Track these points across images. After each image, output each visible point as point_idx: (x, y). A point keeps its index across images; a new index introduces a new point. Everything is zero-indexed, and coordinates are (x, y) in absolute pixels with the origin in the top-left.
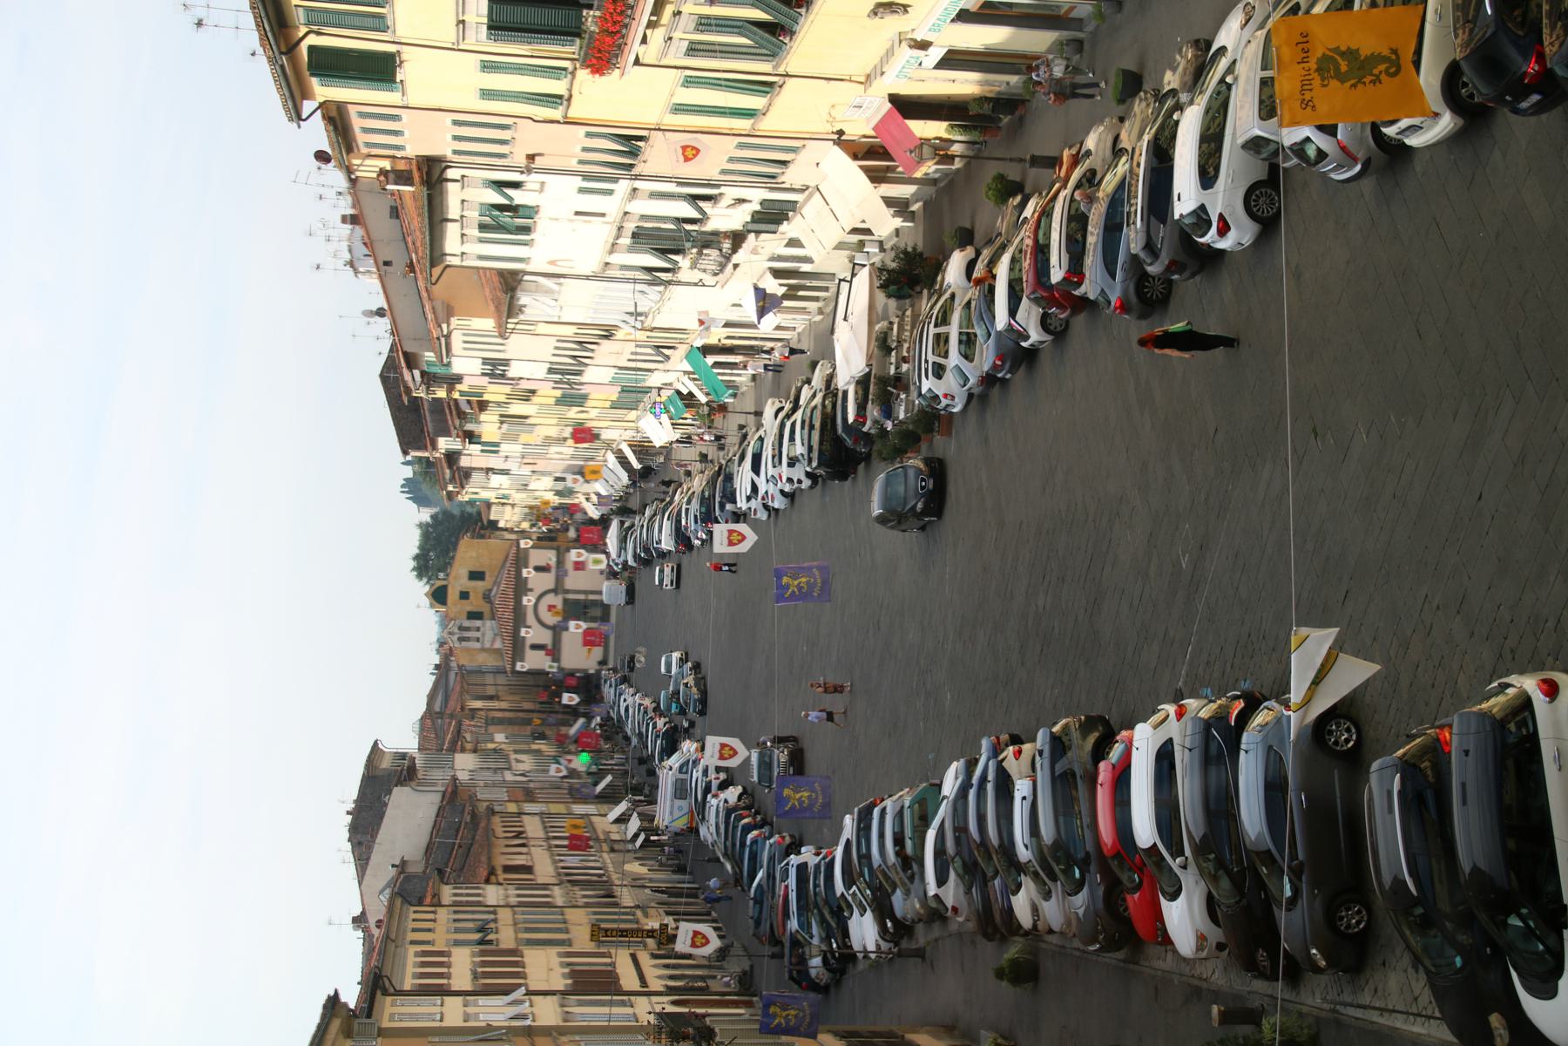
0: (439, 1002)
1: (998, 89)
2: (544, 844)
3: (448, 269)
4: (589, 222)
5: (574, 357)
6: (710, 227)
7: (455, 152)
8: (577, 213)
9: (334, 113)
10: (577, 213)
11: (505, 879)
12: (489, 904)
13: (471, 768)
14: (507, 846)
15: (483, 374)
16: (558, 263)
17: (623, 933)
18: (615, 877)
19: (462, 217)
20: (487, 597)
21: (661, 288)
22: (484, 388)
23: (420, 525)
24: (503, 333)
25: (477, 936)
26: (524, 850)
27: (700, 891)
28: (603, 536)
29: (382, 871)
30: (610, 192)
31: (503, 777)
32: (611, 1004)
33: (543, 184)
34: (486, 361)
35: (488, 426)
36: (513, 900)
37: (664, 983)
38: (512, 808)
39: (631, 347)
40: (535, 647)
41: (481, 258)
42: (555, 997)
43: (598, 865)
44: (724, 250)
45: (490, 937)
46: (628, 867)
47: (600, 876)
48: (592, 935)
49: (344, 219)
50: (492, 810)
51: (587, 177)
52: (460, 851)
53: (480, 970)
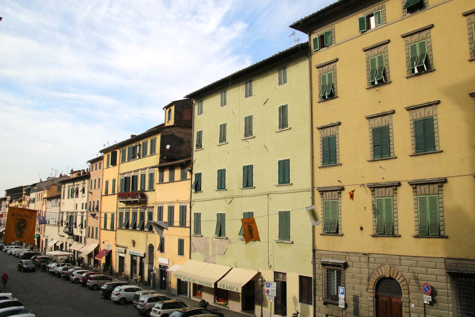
1: (114, 269)
4: (74, 207)
7: (92, 181)
8: (77, 204)
9: (101, 158)
10: (77, 204)
15: (30, 199)
16: (63, 204)
19: (75, 185)
34: (34, 199)
41: (64, 191)
51: (86, 204)
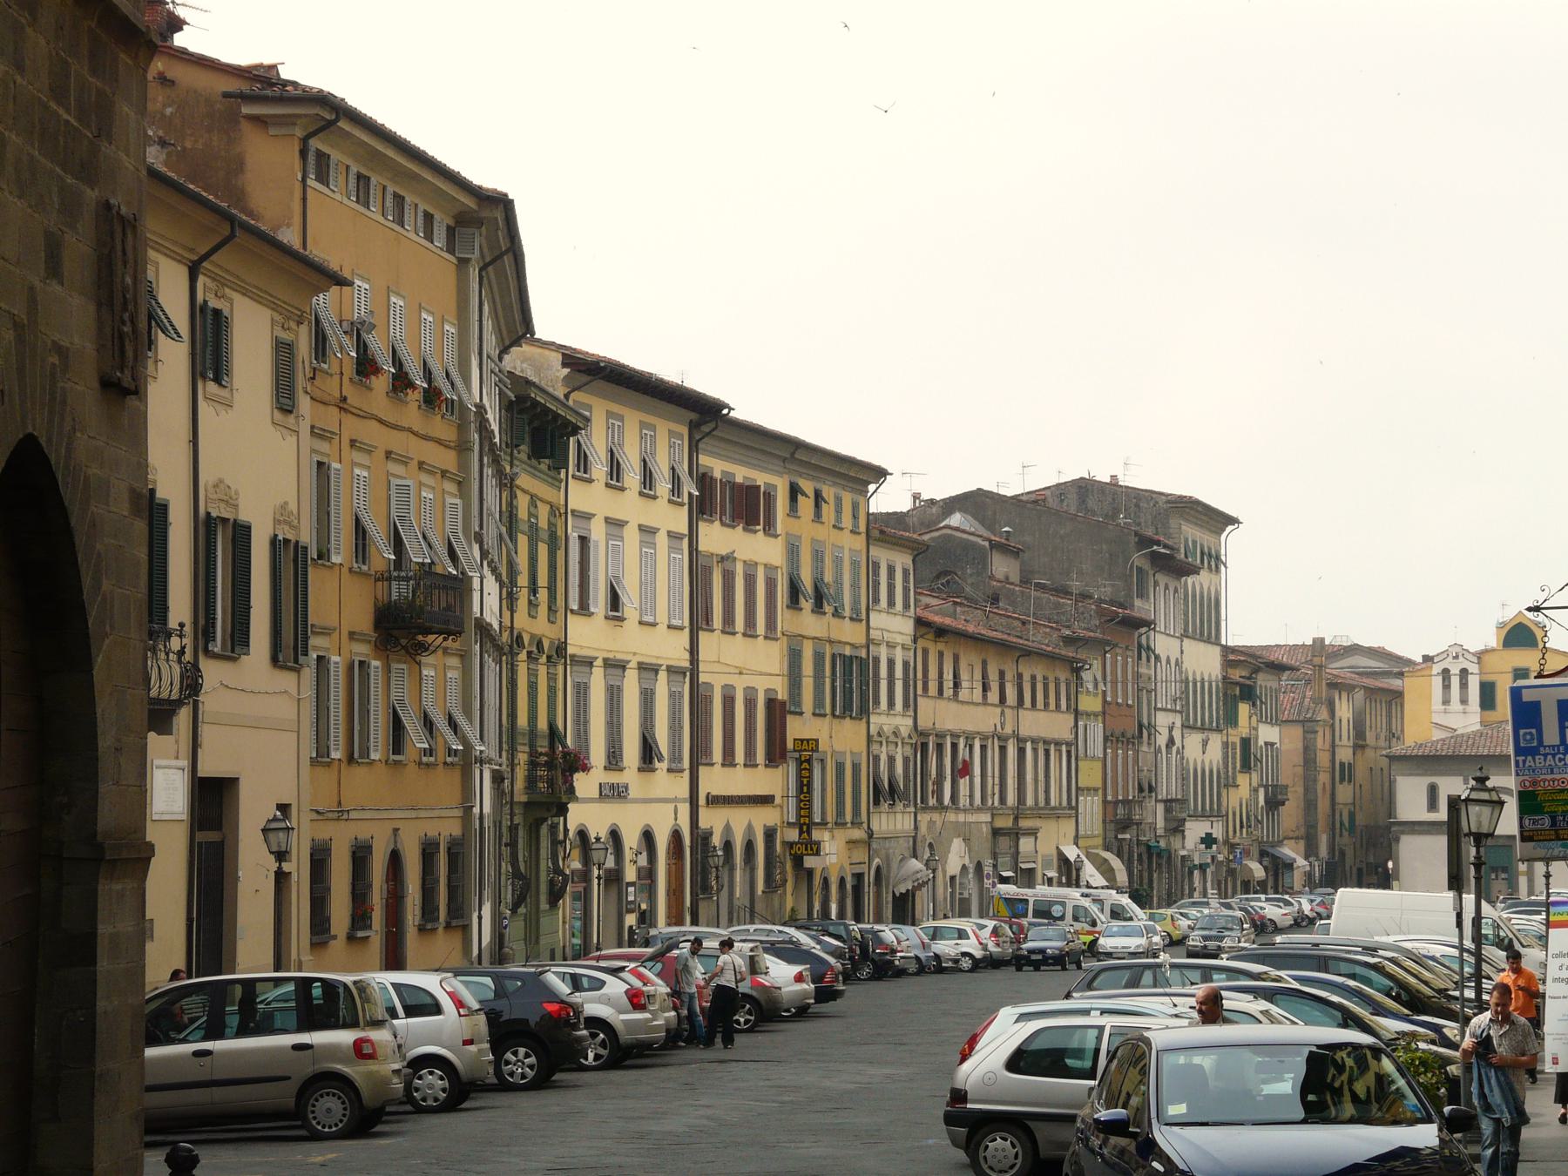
26: (993, 696)
46: (957, 846)
48: (802, 741)
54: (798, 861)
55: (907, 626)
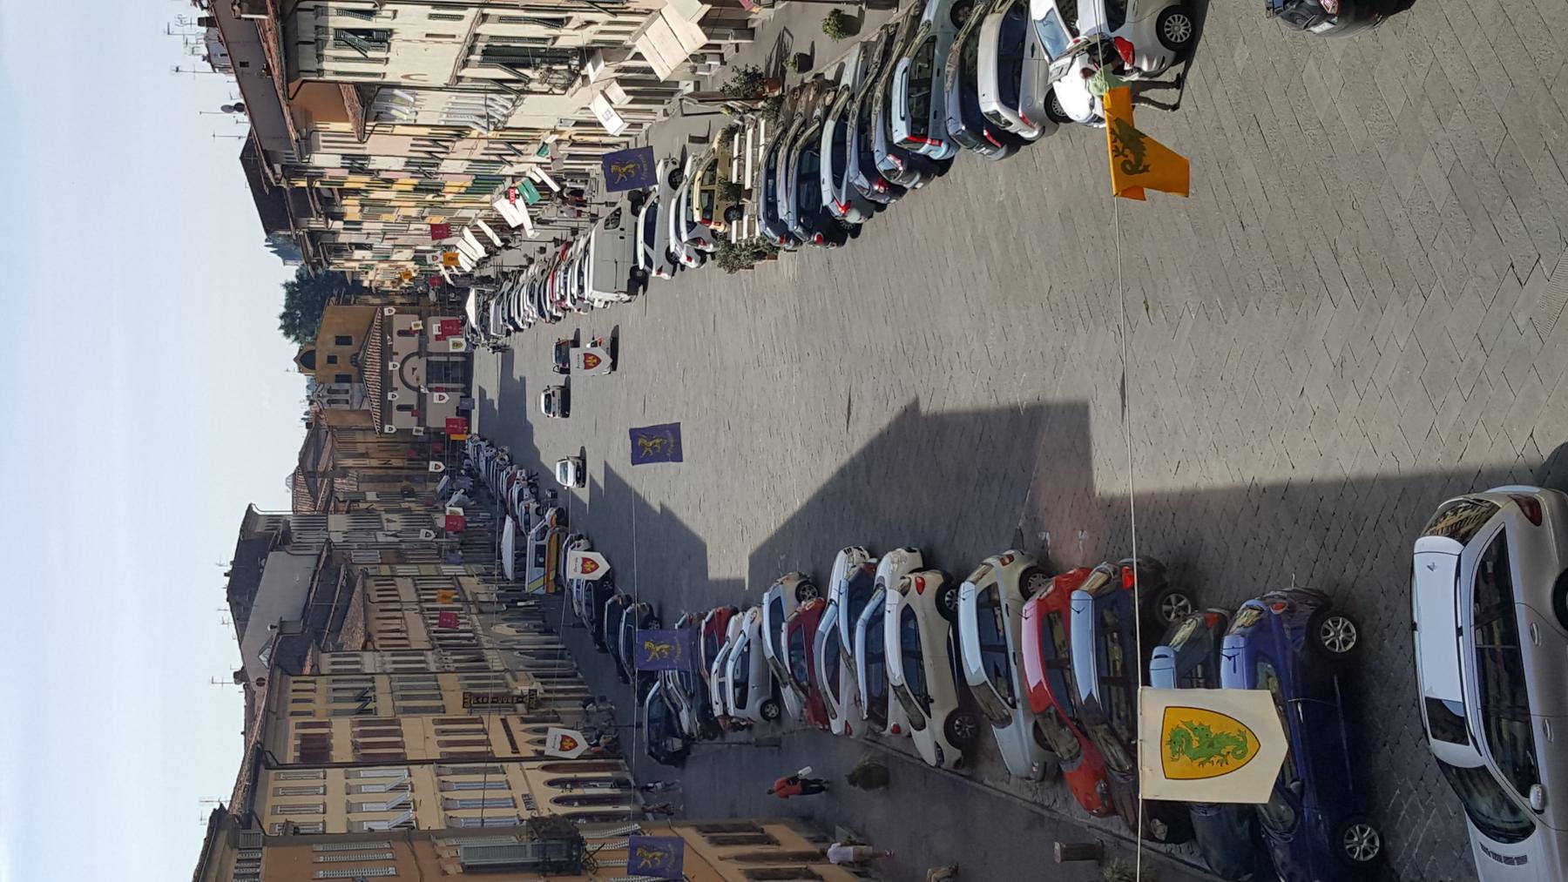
0: (322, 775)
2: (417, 607)
3: (304, 85)
5: (430, 152)
6: (560, 44)
8: (427, 35)
10: (427, 35)
11: (382, 646)
12: (367, 671)
13: (345, 529)
14: (382, 610)
15: (342, 167)
17: (496, 699)
18: (484, 640)
20: (354, 360)
21: (513, 97)
22: (345, 178)
23: (286, 285)
24: (363, 136)
25: (357, 705)
26: (399, 614)
27: (566, 652)
28: (463, 303)
29: (263, 629)
30: (460, 18)
31: (376, 537)
32: (485, 771)
33: (395, 12)
34: (344, 157)
35: (351, 208)
36: (390, 667)
37: (535, 748)
38: (385, 570)
39: (484, 143)
40: (400, 408)
41: (337, 73)
42: (432, 766)
43: (468, 627)
44: (573, 67)
45: (370, 706)
47: (469, 639)
49: (201, 22)
50: (367, 573)
52: (337, 613)
53: (360, 740)
54: (540, 702)
55: (366, 654)
